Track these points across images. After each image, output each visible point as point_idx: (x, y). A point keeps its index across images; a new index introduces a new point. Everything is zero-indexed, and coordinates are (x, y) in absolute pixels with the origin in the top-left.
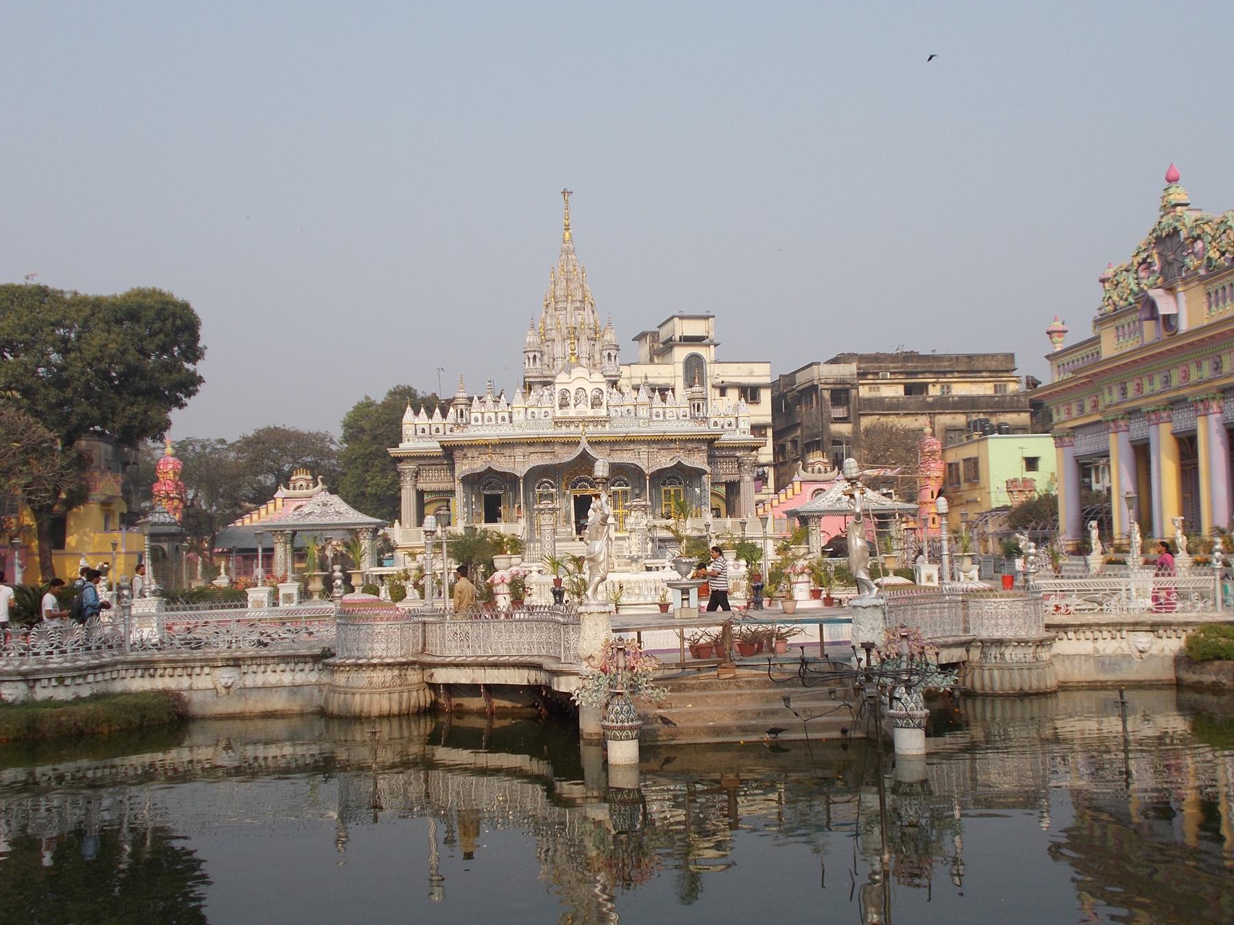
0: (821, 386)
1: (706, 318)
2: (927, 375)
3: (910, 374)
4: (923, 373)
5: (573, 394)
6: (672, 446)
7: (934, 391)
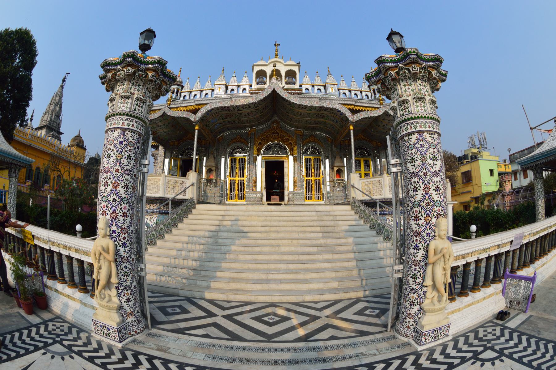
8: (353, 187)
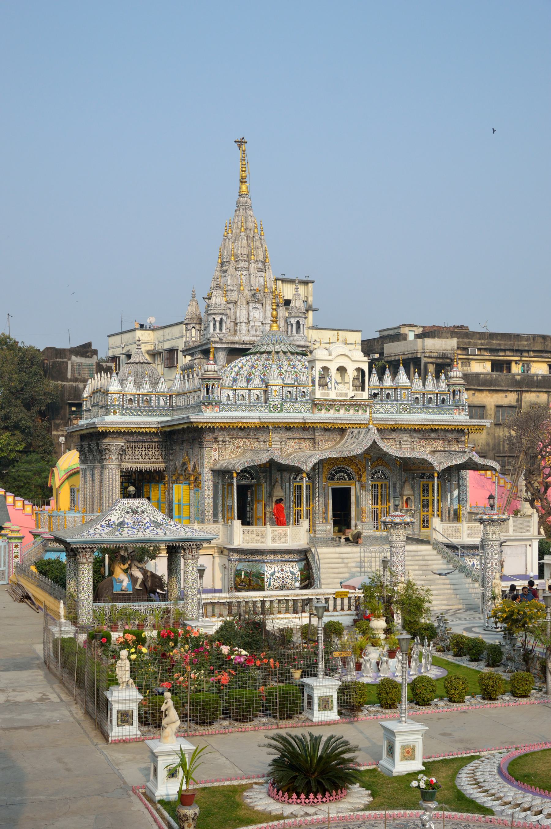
0: (424, 360)
1: (305, 283)
2: (508, 353)
3: (493, 351)
4: (504, 350)
6: (433, 435)
7: (516, 369)
8: (435, 530)
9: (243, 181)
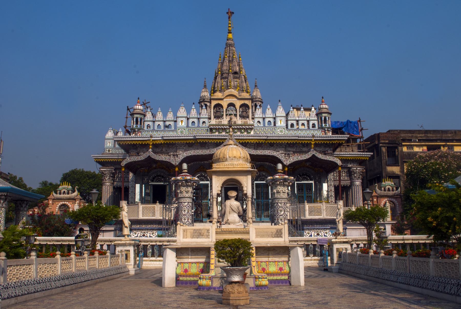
5: (225, 106)
9: (230, 32)
